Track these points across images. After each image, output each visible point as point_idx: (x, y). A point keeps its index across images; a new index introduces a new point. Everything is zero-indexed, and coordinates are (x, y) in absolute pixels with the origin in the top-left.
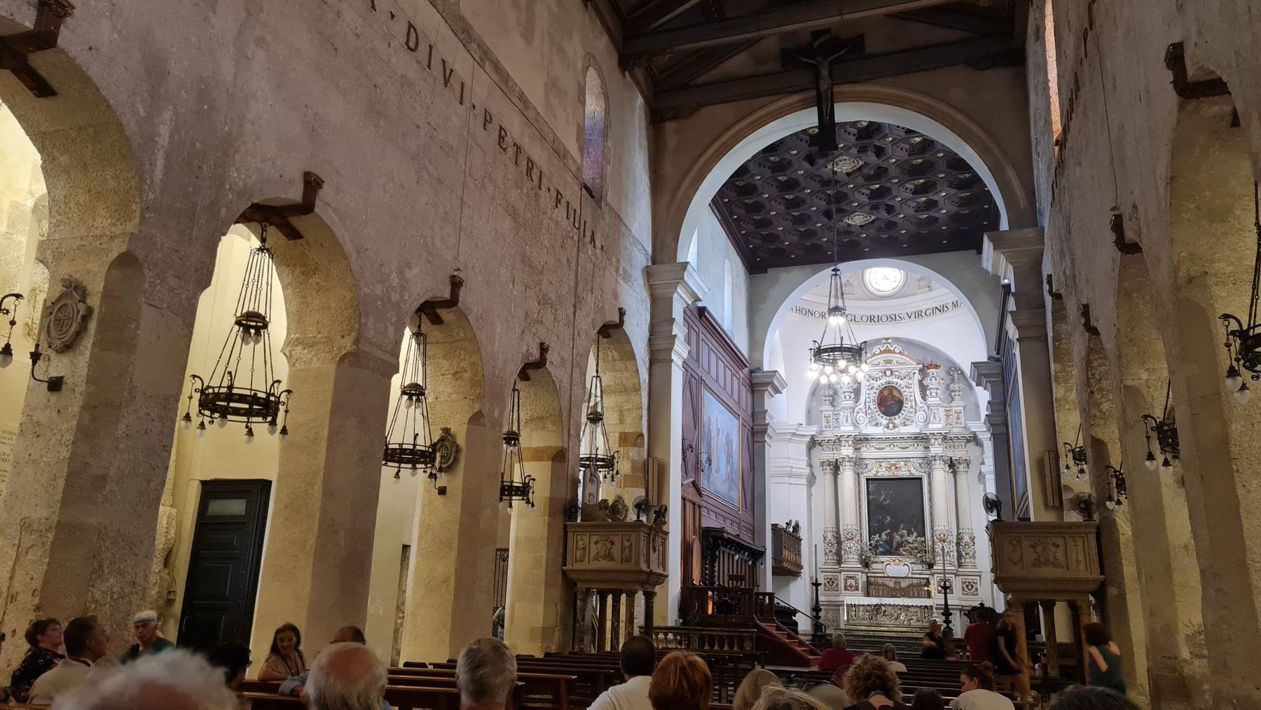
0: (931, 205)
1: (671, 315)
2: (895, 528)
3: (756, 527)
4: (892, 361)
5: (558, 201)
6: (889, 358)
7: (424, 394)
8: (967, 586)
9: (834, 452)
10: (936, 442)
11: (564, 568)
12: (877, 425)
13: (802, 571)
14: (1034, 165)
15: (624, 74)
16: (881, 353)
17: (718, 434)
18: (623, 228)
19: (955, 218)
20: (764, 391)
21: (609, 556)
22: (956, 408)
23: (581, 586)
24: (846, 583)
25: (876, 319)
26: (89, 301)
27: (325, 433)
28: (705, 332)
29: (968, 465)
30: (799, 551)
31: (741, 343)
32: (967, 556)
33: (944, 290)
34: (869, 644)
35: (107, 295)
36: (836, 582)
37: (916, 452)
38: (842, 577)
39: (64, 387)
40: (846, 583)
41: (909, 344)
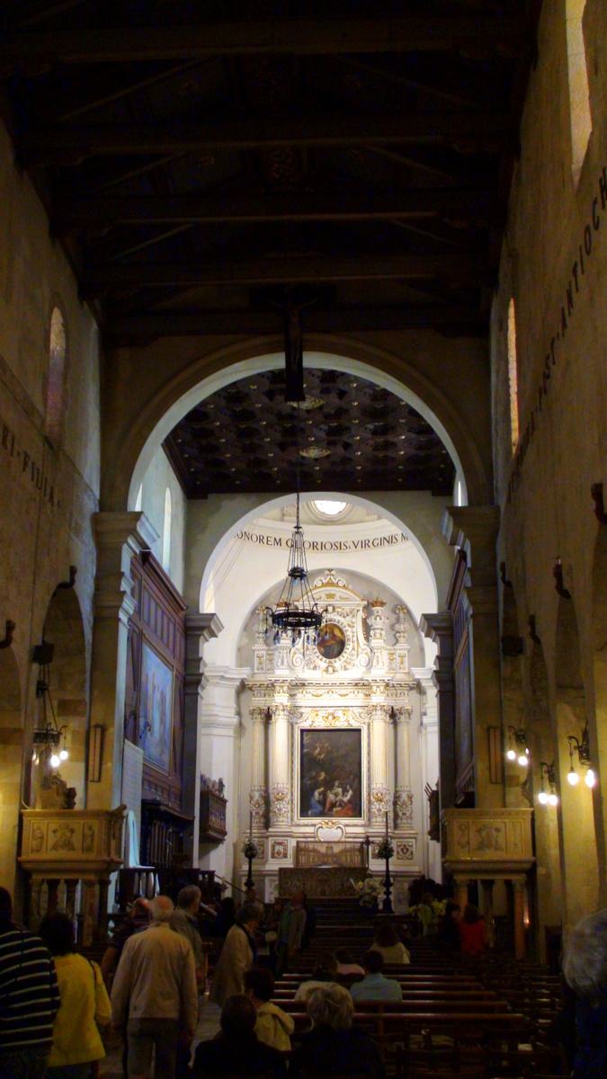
1: (120, 568)
2: (329, 785)
3: (185, 796)
4: (334, 595)
5: (26, 464)
6: (333, 592)
8: (402, 850)
9: (267, 698)
10: (378, 690)
11: (19, 859)
12: (315, 668)
13: (226, 837)
14: (494, 441)
15: (82, 304)
16: (323, 585)
17: (154, 691)
18: (76, 475)
19: (410, 459)
20: (200, 635)
21: (69, 845)
22: (401, 652)
23: (36, 877)
24: (273, 850)
25: (319, 547)
28: (148, 580)
29: (409, 714)
30: (224, 815)
31: (177, 582)
32: (404, 817)
37: (357, 699)
38: (271, 841)
40: (273, 850)
41: (353, 576)
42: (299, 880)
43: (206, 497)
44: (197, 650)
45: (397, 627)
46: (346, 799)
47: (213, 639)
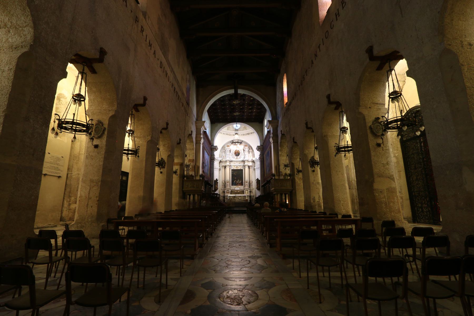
0: (252, 112)
2: (237, 180)
7: (159, 150)
11: (183, 190)
18: (192, 112)
26: (104, 126)
27: (145, 159)
33: (251, 129)
35: (109, 124)
37: (242, 164)
39: (99, 147)
43: (215, 123)
44: (213, 153)
45: (249, 150)
46: (240, 182)
47: (216, 151)
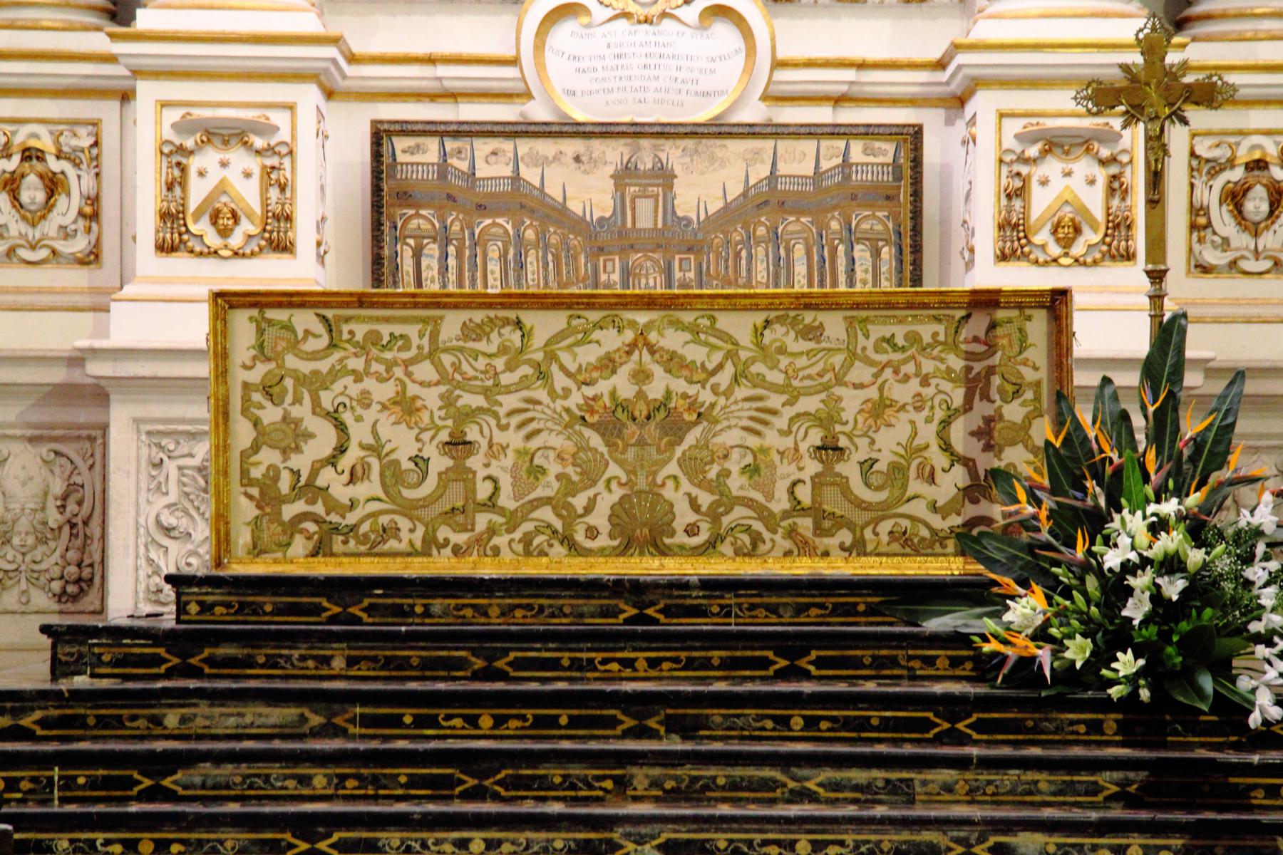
8: (1235, 197)
24: (176, 182)
34: (440, 788)
36: (79, 183)
40: (176, 182)
42: (406, 407)
